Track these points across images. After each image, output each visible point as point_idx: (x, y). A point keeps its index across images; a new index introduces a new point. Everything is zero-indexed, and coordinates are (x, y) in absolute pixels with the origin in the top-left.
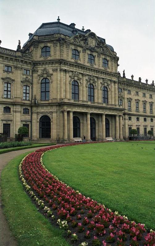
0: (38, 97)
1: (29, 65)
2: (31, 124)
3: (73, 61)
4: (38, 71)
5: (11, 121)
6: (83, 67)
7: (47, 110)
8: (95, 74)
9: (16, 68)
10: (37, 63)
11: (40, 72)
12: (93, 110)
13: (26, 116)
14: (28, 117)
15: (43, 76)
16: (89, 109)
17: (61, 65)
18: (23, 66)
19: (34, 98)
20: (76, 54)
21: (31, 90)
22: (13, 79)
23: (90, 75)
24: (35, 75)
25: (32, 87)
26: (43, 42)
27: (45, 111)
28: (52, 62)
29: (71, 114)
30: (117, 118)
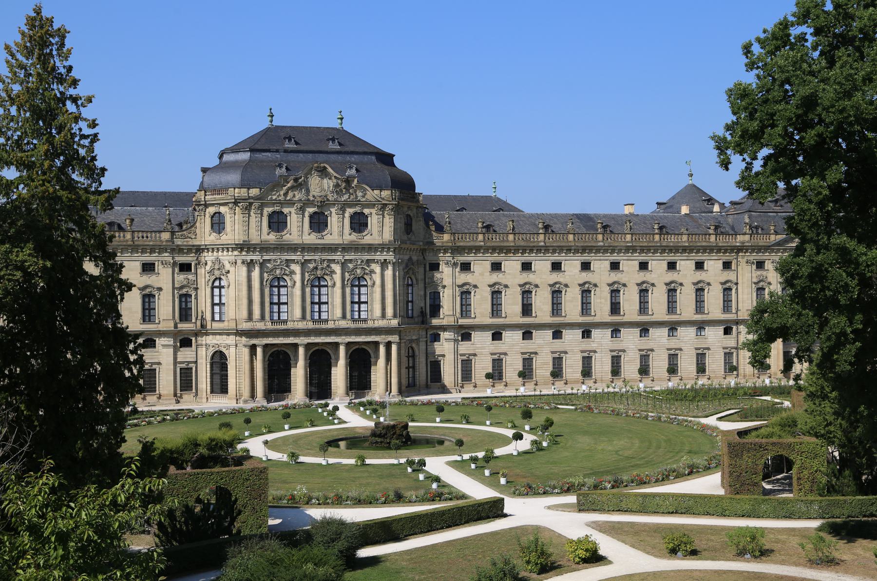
0: (208, 316)
3: (272, 237)
4: (206, 264)
5: (159, 364)
6: (293, 248)
7: (221, 342)
11: (208, 268)
17: (244, 253)
18: (177, 259)
19: (199, 318)
20: (277, 222)
22: (159, 286)
24: (201, 271)
25: (197, 295)
26: (213, 205)
27: (218, 343)
28: (226, 248)
29: (259, 350)
30: (382, 349)
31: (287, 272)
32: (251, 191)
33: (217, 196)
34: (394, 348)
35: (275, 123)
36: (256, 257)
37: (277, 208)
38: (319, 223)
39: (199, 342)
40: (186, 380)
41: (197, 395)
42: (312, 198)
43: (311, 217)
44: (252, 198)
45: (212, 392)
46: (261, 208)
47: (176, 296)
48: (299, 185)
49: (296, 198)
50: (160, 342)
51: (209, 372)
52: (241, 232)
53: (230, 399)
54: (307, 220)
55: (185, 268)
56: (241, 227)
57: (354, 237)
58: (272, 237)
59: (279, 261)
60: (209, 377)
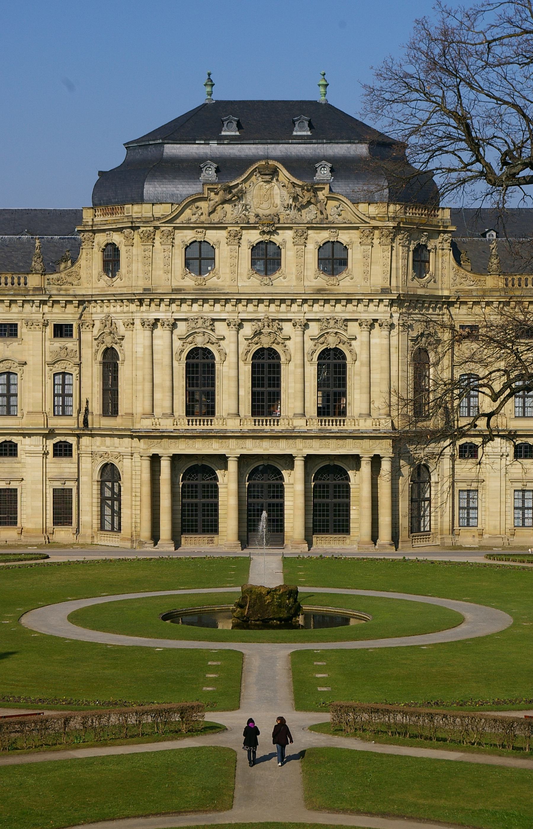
1: (70, 308)
2: (78, 489)
8: (278, 312)
9: (29, 323)
10: (89, 302)
11: (96, 332)
12: (249, 443)
13: (63, 465)
14: (66, 467)
15: (103, 343)
16: (232, 442)
17: (144, 308)
18: (47, 317)
19: (83, 410)
21: (76, 383)
22: (24, 359)
23: (259, 320)
24: (87, 337)
25: (80, 373)
29: (165, 466)
31: (214, 340)
32: (157, 208)
33: (108, 218)
34: (386, 466)
35: (216, 97)
36: (163, 313)
37: (199, 237)
38: (266, 259)
39: (83, 448)
40: (63, 508)
41: (78, 531)
42: (252, 220)
43: (254, 249)
44: (159, 219)
45: (102, 528)
46: (171, 235)
47: (49, 374)
48: (234, 196)
49: (229, 218)
50: (24, 444)
51: (95, 496)
52: (141, 275)
53: (123, 539)
54: (246, 253)
55: (62, 331)
56: (140, 265)
57: (322, 281)
58: (190, 282)
59: (200, 321)
60: (95, 504)
